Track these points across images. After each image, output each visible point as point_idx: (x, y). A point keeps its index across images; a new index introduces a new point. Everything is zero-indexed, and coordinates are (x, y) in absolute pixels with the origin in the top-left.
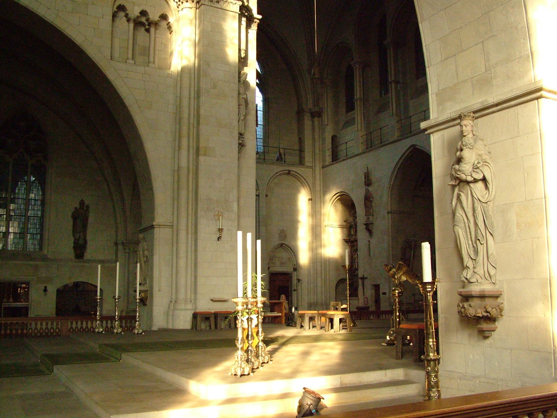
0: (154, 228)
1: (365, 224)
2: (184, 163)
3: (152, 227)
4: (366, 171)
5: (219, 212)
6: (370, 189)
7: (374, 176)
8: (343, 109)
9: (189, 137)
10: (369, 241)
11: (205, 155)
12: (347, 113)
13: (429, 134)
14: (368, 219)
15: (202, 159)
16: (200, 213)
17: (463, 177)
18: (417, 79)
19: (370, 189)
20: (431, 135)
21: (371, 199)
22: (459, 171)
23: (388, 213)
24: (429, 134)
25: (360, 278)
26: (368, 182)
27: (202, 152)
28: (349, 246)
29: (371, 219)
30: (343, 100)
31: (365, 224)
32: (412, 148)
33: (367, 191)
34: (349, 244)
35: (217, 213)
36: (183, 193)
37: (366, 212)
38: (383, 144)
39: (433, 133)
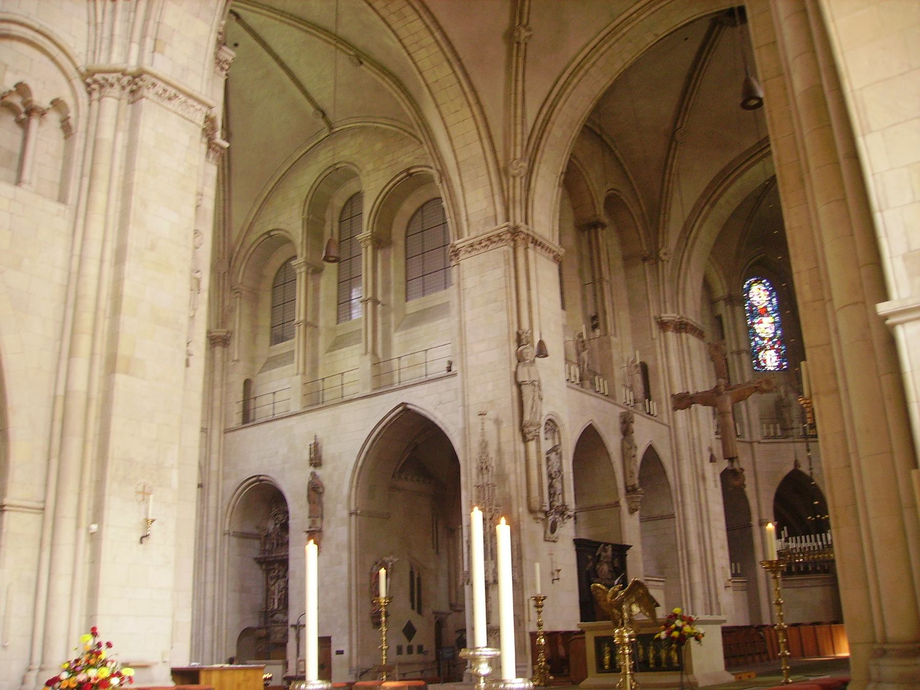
1: (307, 532)
2: (79, 383)
5: (144, 486)
6: (319, 472)
7: (327, 451)
8: (264, 338)
9: (94, 336)
11: (126, 372)
12: (271, 345)
14: (314, 522)
15: (120, 379)
16: (111, 486)
18: (407, 300)
19: (319, 472)
21: (321, 490)
23: (351, 514)
25: (292, 626)
26: (316, 461)
27: (120, 364)
28: (264, 570)
29: (318, 524)
30: (265, 321)
32: (401, 408)
33: (313, 475)
35: (140, 488)
36: (74, 444)
37: (311, 511)
38: (346, 398)
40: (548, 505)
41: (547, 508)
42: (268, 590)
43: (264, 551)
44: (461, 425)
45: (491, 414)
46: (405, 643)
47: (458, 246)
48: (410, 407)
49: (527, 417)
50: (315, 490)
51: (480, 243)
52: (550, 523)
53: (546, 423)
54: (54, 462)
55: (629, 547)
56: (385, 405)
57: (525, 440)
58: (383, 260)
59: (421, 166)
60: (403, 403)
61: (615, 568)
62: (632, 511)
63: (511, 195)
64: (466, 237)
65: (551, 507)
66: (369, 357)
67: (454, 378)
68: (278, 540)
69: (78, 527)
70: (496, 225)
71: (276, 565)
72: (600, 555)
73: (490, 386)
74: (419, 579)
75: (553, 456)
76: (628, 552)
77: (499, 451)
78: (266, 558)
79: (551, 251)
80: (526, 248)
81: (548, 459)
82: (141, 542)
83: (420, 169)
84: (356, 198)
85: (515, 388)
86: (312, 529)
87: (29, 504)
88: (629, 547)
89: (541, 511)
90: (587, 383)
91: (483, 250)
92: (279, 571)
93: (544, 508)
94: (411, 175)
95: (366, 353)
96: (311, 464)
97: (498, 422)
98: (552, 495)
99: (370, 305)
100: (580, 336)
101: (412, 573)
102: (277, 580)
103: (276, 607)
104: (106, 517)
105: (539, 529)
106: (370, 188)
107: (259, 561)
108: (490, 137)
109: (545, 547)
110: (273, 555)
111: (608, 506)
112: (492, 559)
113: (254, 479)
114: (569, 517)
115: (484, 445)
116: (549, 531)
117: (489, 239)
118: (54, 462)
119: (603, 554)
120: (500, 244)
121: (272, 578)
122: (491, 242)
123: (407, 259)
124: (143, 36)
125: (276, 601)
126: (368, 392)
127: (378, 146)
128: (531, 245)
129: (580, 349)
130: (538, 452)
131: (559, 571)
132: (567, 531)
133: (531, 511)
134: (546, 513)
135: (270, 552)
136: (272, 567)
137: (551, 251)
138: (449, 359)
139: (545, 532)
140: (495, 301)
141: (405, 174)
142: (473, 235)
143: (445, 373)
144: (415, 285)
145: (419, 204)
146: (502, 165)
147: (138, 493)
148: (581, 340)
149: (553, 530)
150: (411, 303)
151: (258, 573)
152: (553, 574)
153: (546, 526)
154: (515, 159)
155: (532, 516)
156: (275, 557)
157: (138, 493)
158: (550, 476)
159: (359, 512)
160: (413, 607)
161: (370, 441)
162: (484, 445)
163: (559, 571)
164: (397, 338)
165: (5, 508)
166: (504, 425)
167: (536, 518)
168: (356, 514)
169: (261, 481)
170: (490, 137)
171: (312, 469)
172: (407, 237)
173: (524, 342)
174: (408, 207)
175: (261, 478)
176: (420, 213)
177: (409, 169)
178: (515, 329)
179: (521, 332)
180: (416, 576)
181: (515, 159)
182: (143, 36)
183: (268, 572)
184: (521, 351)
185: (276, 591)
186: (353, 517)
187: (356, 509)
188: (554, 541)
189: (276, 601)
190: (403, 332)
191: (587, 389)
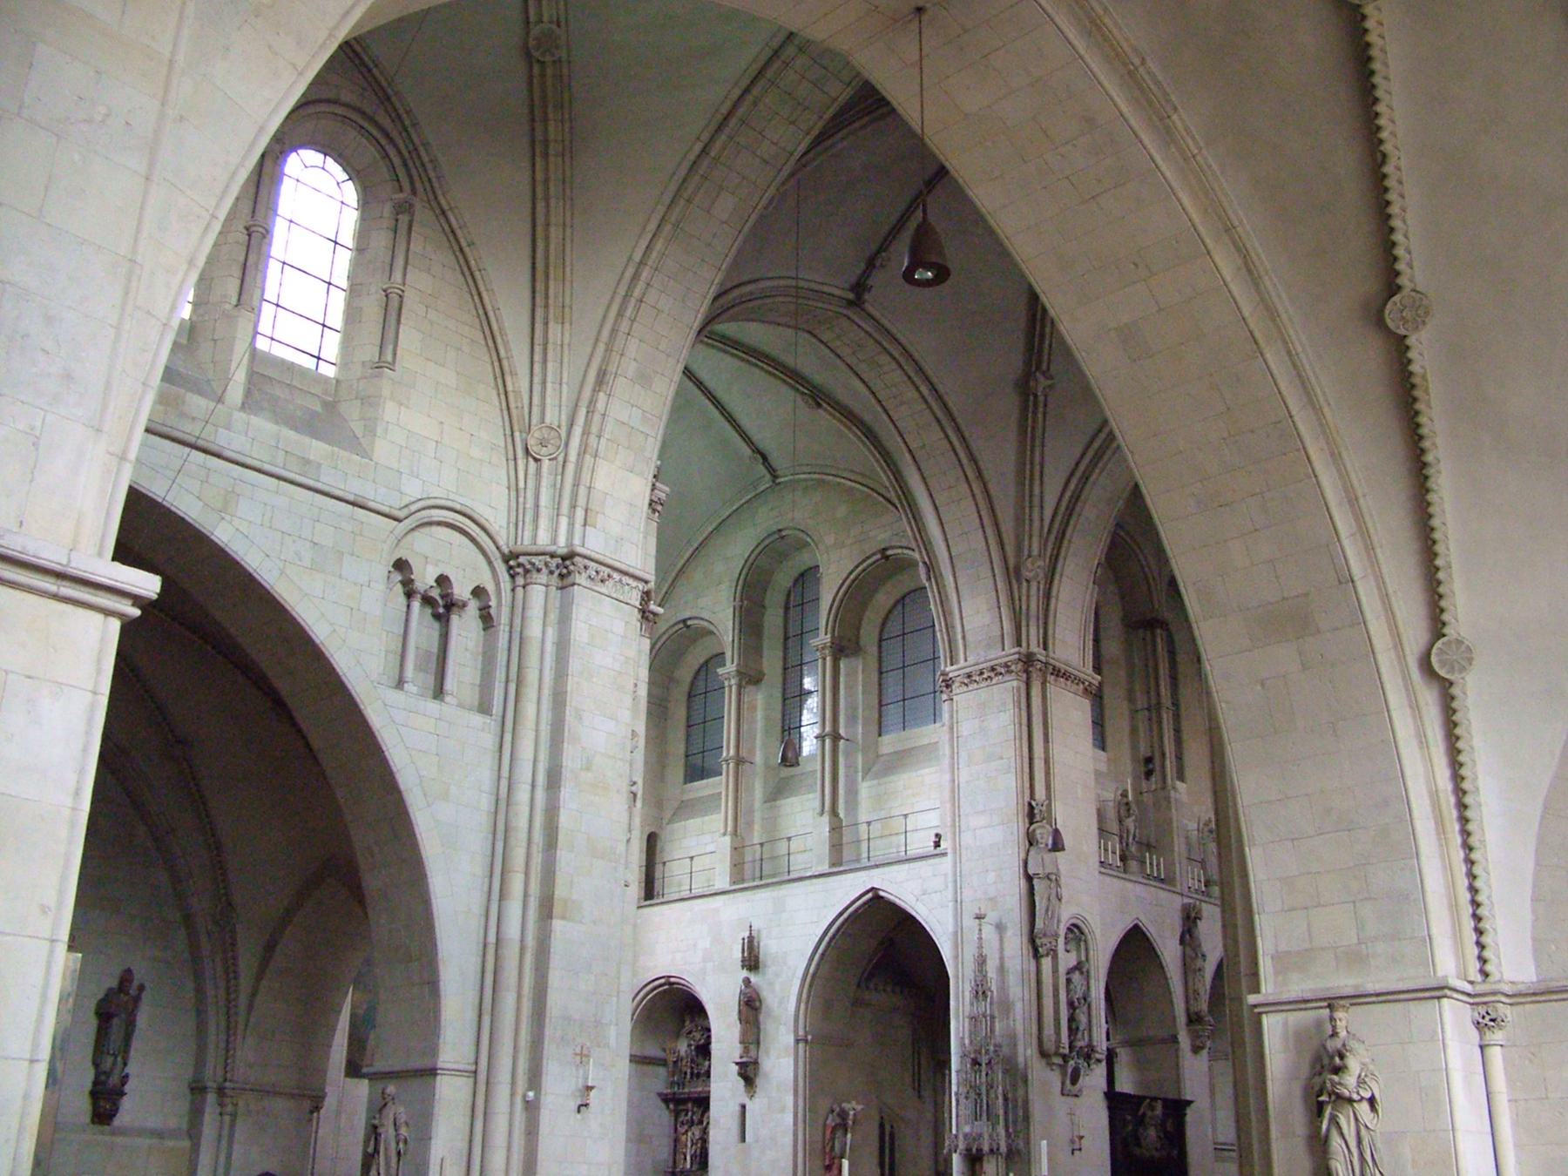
0: (436, 1075)
1: (737, 1064)
2: (512, 930)
3: (432, 1072)
4: (747, 934)
5: (582, 1047)
6: (753, 979)
8: (677, 771)
9: (527, 874)
10: (743, 1107)
11: (563, 918)
12: (685, 783)
13: (1260, 1014)
14: (746, 1050)
15: (558, 925)
16: (549, 1048)
17: (1346, 1093)
18: (880, 735)
20: (1264, 1016)
21: (757, 1004)
22: (1340, 1084)
23: (797, 1041)
24: (1260, 1014)
26: (752, 961)
27: (557, 910)
28: (671, 1111)
29: (753, 1053)
30: (678, 748)
31: (737, 1064)
32: (870, 895)
33: (747, 981)
34: (671, 1106)
35: (578, 1050)
36: (508, 1000)
38: (793, 876)
39: (1266, 1013)
40: (1067, 1046)
41: (1067, 1051)
42: (676, 1141)
43: (672, 1084)
44: (951, 929)
45: (992, 917)
47: (951, 675)
48: (882, 893)
49: (1039, 924)
50: (751, 1006)
51: (982, 673)
52: (1070, 1070)
53: (1069, 929)
54: (486, 1019)
55: (1189, 1103)
56: (847, 890)
57: (1037, 955)
58: (847, 675)
59: (901, 547)
60: (873, 889)
61: (1166, 1132)
62: (1196, 1049)
63: (1024, 607)
64: (962, 663)
65: (1071, 1047)
66: (826, 818)
67: (944, 859)
68: (692, 1068)
69: (513, 1095)
70: (1003, 650)
71: (690, 1105)
72: (1144, 1114)
73: (991, 877)
74: (892, 1136)
75: (1076, 977)
76: (1189, 1111)
77: (1002, 969)
78: (674, 1094)
79: (1078, 681)
80: (1044, 683)
81: (1069, 981)
82: (579, 1111)
83: (899, 551)
84: (807, 578)
85: (1023, 882)
86: (744, 1060)
87: (461, 1067)
88: (1189, 1103)
89: (1057, 1054)
90: (1133, 865)
91: (984, 684)
92: (693, 1113)
93: (1061, 1050)
94: (887, 558)
95: (822, 813)
96: (743, 967)
97: (1000, 928)
98: (1073, 1031)
99: (828, 741)
100: (1124, 795)
101: (882, 1126)
102: (690, 1127)
103: (688, 1166)
104: (544, 1084)
105: (1055, 1078)
106: (830, 571)
107: (666, 1099)
108: (997, 525)
109: (1061, 1104)
110: (686, 1090)
111: (1163, 1041)
112: (988, 1120)
113: (663, 981)
114: (1099, 1061)
115: (981, 961)
116: (1068, 1082)
117: (993, 669)
118: (486, 1019)
119: (1149, 1113)
120: (1007, 677)
121: (682, 1123)
122: (996, 675)
123: (881, 673)
124: (573, 507)
125: (688, 1158)
126: (825, 868)
127: (842, 511)
128: (1051, 678)
129: (1123, 812)
130: (1055, 971)
131: (1081, 1138)
132: (1095, 1079)
133: (1044, 1054)
134: (1064, 1057)
135: (681, 1084)
136: (681, 1107)
137: (1078, 681)
138: (935, 831)
139: (1063, 1083)
140: (1002, 758)
141: (879, 556)
142: (971, 660)
143: (931, 849)
144: (893, 712)
145: (897, 594)
146: (1012, 562)
147: (576, 1054)
148: (1125, 800)
149: (1074, 1080)
150: (886, 739)
151: (664, 1116)
152: (1072, 1142)
153: (1064, 1074)
154: (1029, 556)
155: (1044, 1062)
156: (690, 1093)
157: (576, 1054)
158: (1071, 1005)
159: (809, 1037)
161: (827, 939)
162: (981, 961)
163: (1081, 1138)
164: (865, 789)
165: (439, 1072)
166: (1009, 933)
167: (1050, 1064)
168: (806, 1041)
169: (671, 984)
170: (997, 525)
171: (745, 973)
172: (880, 640)
173: (1038, 818)
174: (883, 599)
175: (672, 980)
176: (900, 607)
177: (885, 549)
178: (1027, 799)
179: (1034, 803)
180: (888, 1128)
181: (1029, 556)
182: (573, 507)
183: (677, 1114)
184: (1034, 830)
185: (689, 1144)
186: (801, 1045)
187: (806, 1033)
188: (1076, 1096)
189: (688, 1158)
190: (875, 782)
191: (1132, 873)
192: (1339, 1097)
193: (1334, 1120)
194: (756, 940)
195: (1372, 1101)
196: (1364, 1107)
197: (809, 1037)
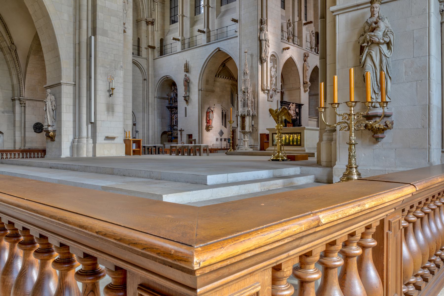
0: (61, 85)
1: (184, 97)
3: (59, 84)
4: (186, 63)
10: (186, 108)
13: (335, 15)
14: (186, 93)
17: (377, 40)
18: (221, 6)
20: (337, 17)
22: (374, 36)
23: (199, 90)
24: (335, 15)
25: (179, 130)
26: (187, 69)
28: (170, 111)
29: (188, 94)
31: (184, 97)
33: (186, 75)
34: (170, 110)
37: (185, 89)
39: (338, 15)
40: (269, 87)
42: (171, 118)
43: (170, 104)
45: (250, 52)
46: (219, 137)
48: (220, 49)
50: (187, 82)
53: (271, 56)
55: (303, 105)
56: (212, 48)
61: (296, 112)
62: (305, 91)
65: (271, 88)
67: (237, 38)
68: (174, 100)
71: (174, 109)
72: (290, 107)
74: (225, 115)
76: (302, 107)
78: (170, 106)
85: (258, 41)
86: (185, 96)
88: (303, 105)
89: (267, 90)
90: (291, 40)
92: (175, 111)
93: (268, 88)
96: (185, 71)
97: (252, 55)
100: (289, 20)
101: (222, 113)
102: (175, 115)
103: (174, 124)
107: (168, 108)
110: (173, 105)
112: (247, 107)
113: (165, 77)
114: (278, 92)
121: (173, 114)
125: (174, 122)
126: (205, 43)
129: (288, 26)
134: (268, 90)
135: (172, 104)
136: (173, 110)
148: (289, 22)
149: (271, 97)
150: (223, 7)
151: (168, 112)
153: (268, 96)
155: (262, 92)
156: (174, 106)
160: (223, 125)
167: (264, 93)
169: (167, 78)
171: (185, 73)
173: (263, 23)
175: (167, 77)
178: (260, 17)
179: (262, 19)
180: (224, 114)
183: (171, 111)
185: (174, 119)
186: (200, 91)
188: (272, 101)
189: (174, 122)
191: (291, 43)
192: (373, 43)
193: (369, 55)
194: (188, 64)
195: (389, 44)
196: (384, 48)
197: (202, 89)
